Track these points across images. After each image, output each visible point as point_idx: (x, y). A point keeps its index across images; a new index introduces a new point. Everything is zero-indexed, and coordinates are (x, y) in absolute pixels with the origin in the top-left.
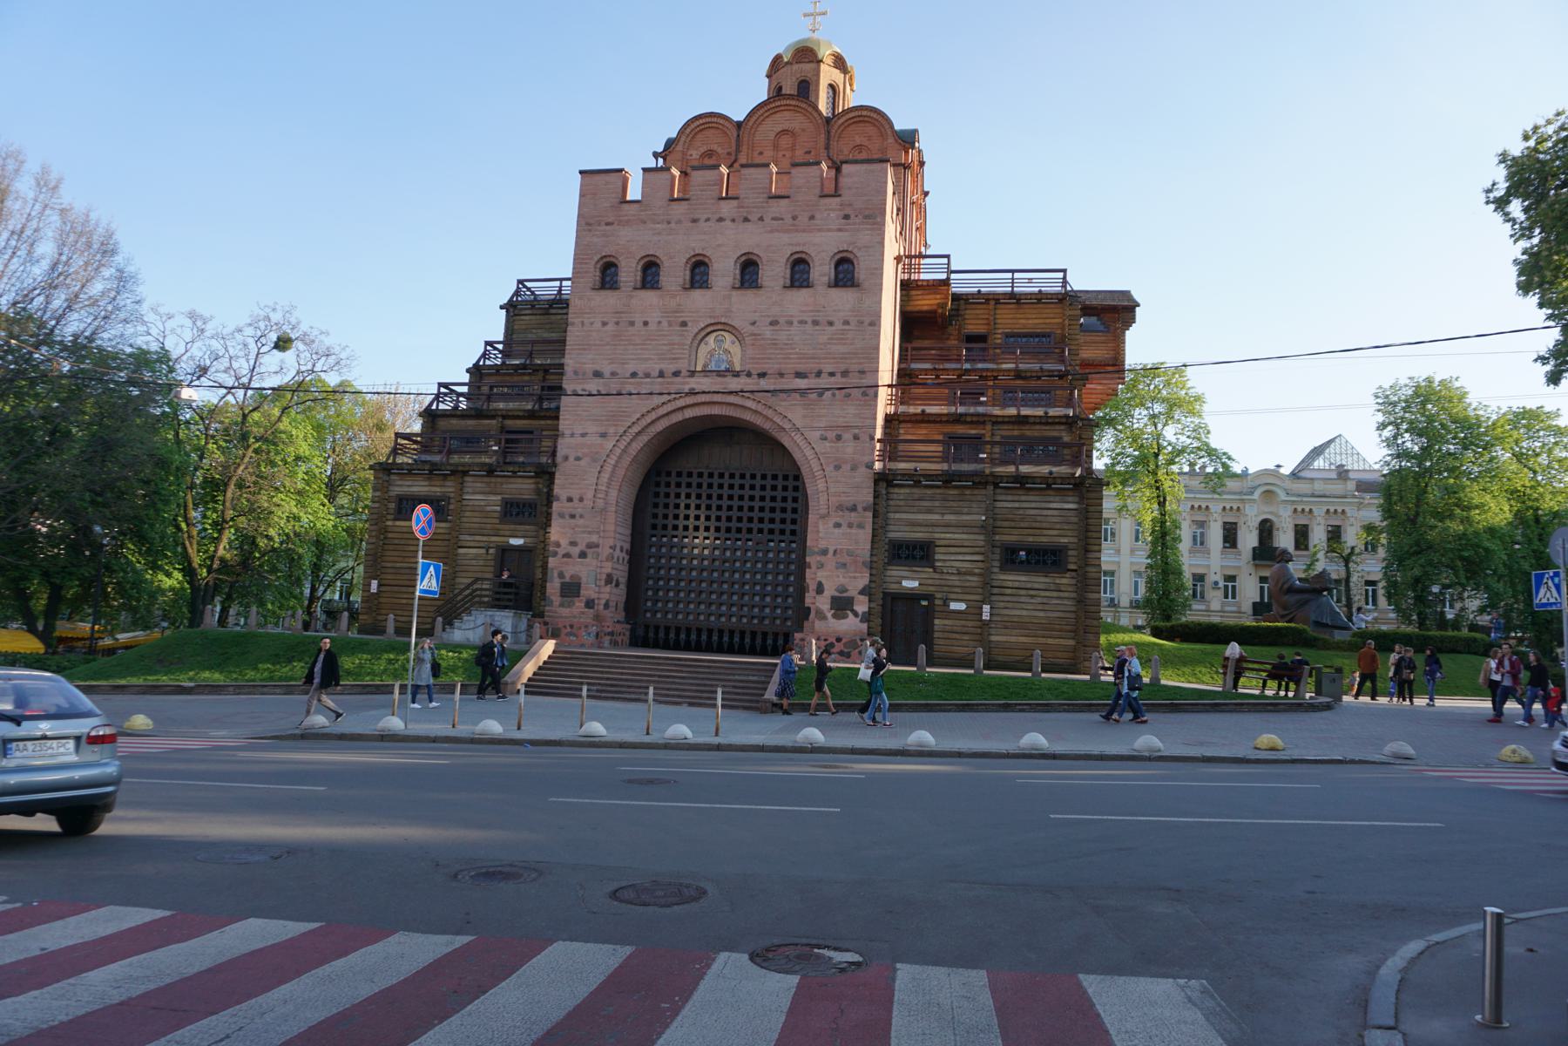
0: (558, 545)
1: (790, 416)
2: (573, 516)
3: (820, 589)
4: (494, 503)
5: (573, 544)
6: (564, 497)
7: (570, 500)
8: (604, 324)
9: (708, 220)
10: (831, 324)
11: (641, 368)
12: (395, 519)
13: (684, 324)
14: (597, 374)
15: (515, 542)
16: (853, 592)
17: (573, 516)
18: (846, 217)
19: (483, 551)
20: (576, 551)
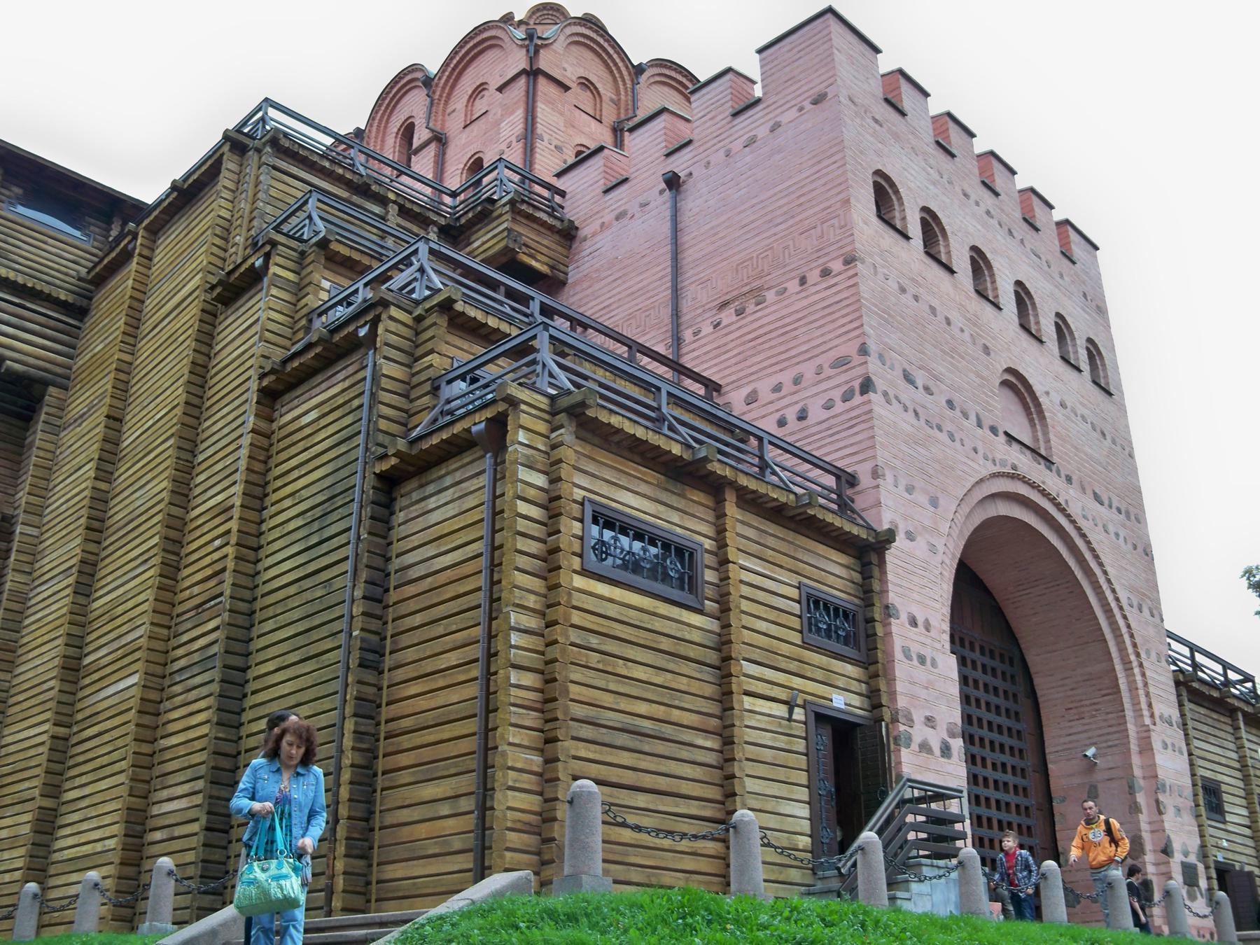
0: (910, 722)
1: (1103, 559)
2: (922, 660)
3: (1166, 851)
4: (785, 588)
5: (930, 721)
6: (904, 617)
7: (913, 622)
8: (903, 290)
9: (977, 204)
10: (1103, 434)
11: (957, 398)
12: (585, 572)
13: (986, 350)
14: (908, 378)
15: (839, 701)
16: (1192, 859)
17: (922, 660)
18: (1085, 295)
19: (781, 710)
20: (934, 739)
